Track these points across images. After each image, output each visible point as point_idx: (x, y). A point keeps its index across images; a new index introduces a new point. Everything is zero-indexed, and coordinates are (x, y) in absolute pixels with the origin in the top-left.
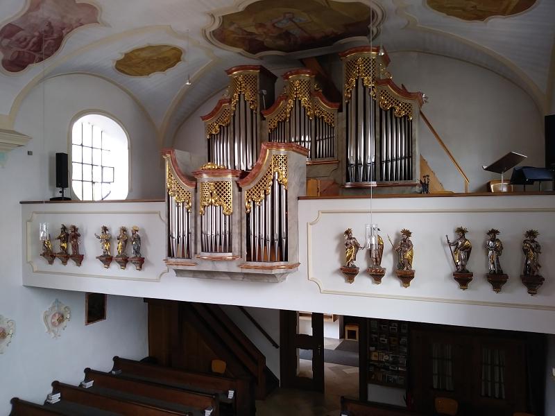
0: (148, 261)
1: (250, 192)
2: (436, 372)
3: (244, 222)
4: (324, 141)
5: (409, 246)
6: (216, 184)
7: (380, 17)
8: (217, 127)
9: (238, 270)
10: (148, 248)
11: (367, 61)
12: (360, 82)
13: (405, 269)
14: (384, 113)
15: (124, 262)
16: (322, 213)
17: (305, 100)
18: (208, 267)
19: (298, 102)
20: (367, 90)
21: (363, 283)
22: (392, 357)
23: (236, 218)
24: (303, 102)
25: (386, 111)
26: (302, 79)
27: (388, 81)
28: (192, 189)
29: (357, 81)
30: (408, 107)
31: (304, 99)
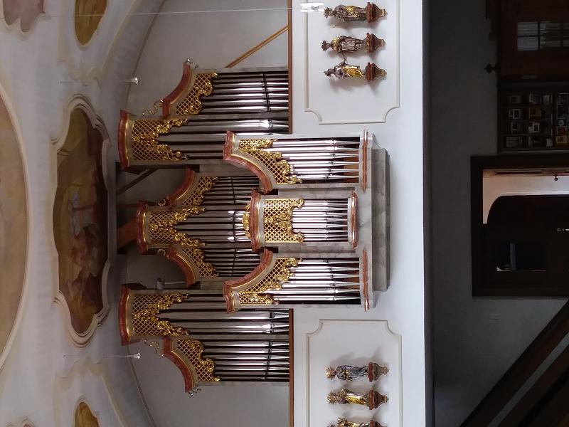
0: (377, 354)
1: (279, 178)
2: (559, 42)
3: (312, 186)
4: (236, 192)
5: (341, 8)
6: (267, 215)
7: (83, 102)
8: (203, 362)
9: (369, 191)
10: (356, 356)
11: (135, 131)
12: (162, 139)
13: (365, 12)
14: (205, 110)
15: (376, 399)
16: (308, 107)
17: (177, 217)
18: (367, 233)
19: (179, 226)
20: (175, 130)
21: (384, 59)
22: (559, 116)
23: (308, 195)
24: (182, 218)
25: (204, 107)
26: (148, 221)
27: (166, 103)
28: (275, 257)
29: (161, 143)
30: (201, 78)
31: (177, 217)
